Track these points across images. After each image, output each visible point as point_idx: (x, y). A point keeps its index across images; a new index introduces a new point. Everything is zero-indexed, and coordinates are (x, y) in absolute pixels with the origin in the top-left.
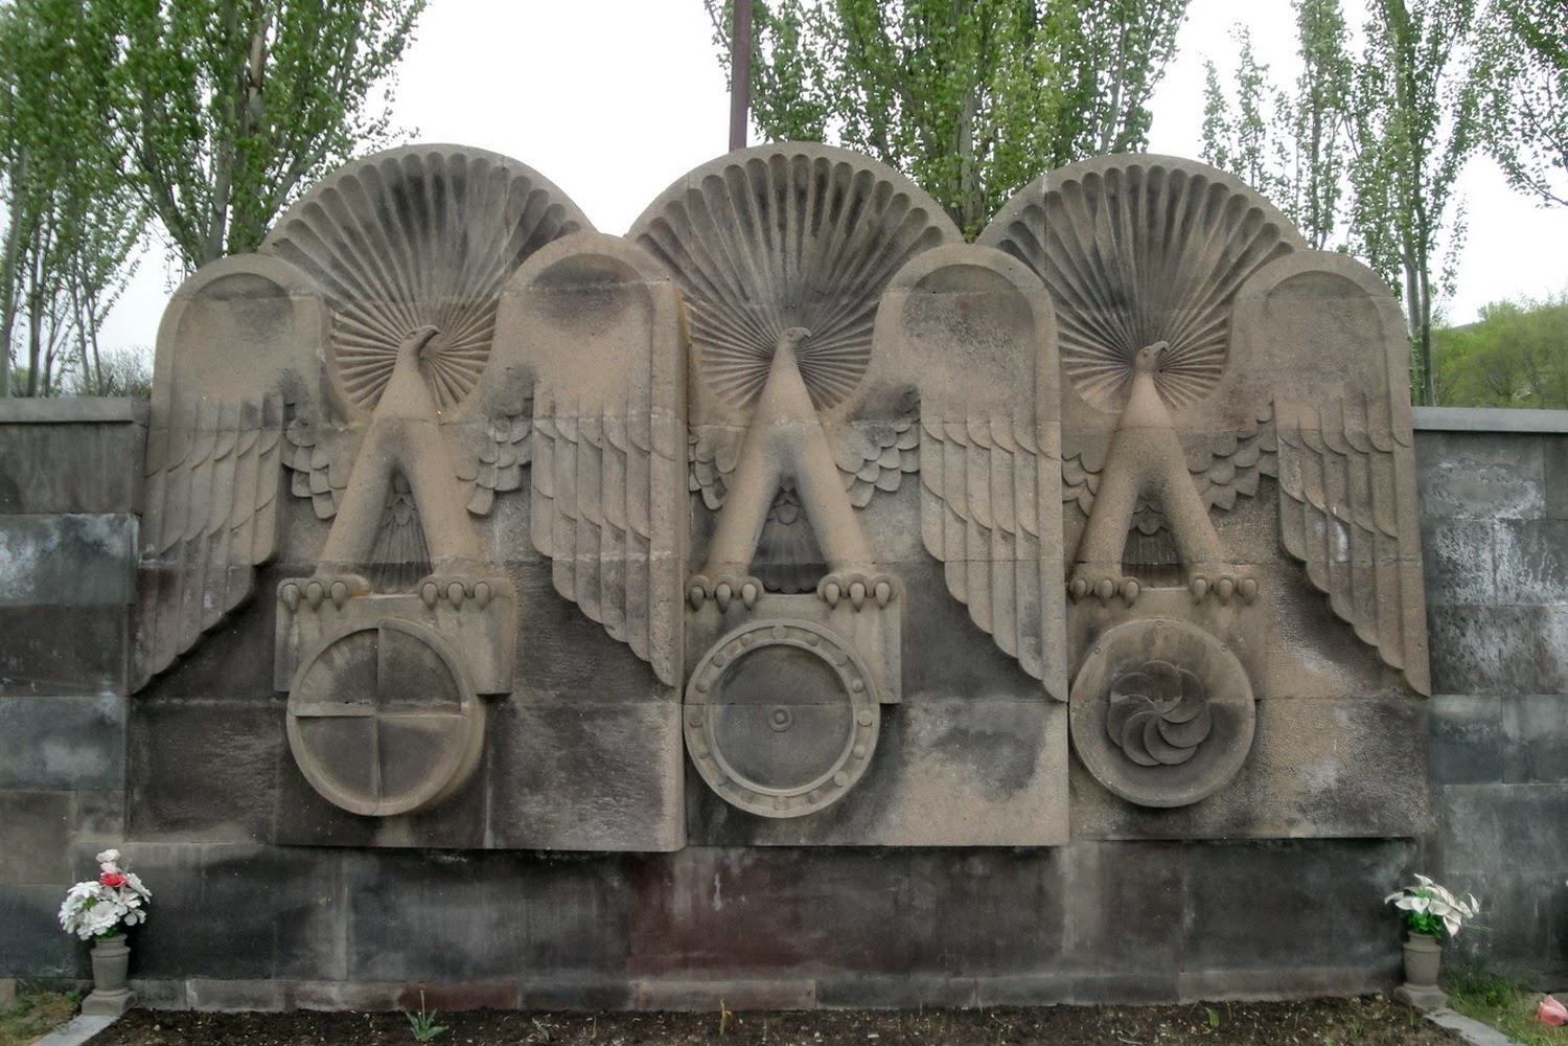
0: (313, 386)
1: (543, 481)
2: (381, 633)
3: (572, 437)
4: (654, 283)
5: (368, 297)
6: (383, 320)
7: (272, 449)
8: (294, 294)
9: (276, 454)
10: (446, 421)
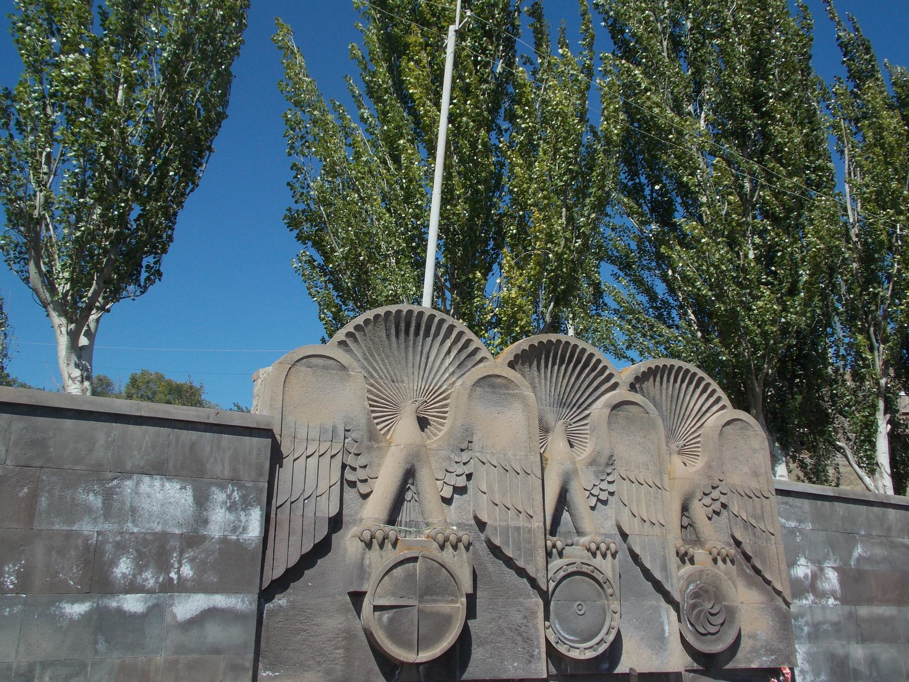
0: (363, 421)
2: (420, 559)
3: (495, 463)
5: (381, 378)
8: (352, 371)
9: (340, 455)
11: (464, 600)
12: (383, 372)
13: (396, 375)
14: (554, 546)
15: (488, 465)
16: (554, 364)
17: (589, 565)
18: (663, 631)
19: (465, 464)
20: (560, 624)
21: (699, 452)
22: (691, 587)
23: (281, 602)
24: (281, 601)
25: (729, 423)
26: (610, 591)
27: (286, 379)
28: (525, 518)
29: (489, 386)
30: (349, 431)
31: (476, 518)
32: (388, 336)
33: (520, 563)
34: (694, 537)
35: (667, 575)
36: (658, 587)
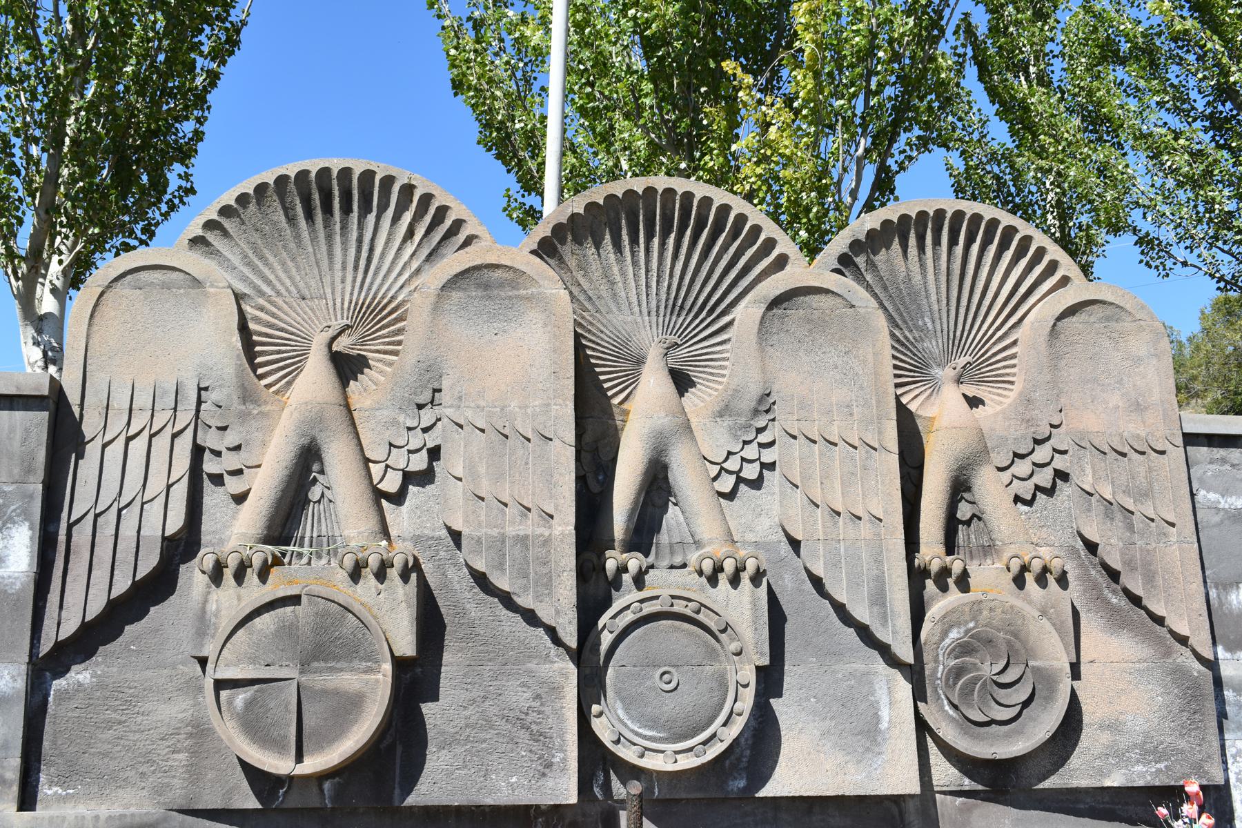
2: (304, 599)
4: (554, 291)
5: (278, 293)
6: (293, 314)
7: (185, 428)
8: (212, 286)
9: (189, 433)
10: (357, 406)
11: (387, 667)
12: (283, 284)
13: (309, 287)
14: (623, 569)
15: (467, 428)
16: (650, 237)
17: (689, 600)
18: (877, 718)
19: (425, 430)
20: (627, 710)
21: (1014, 375)
22: (954, 634)
23: (80, 677)
24: (80, 675)
25: (1072, 311)
26: (734, 647)
27: (94, 311)
28: (537, 519)
29: (478, 286)
30: (206, 389)
31: (449, 529)
32: (291, 220)
33: (524, 601)
34: (985, 541)
35: (885, 612)
36: (865, 633)
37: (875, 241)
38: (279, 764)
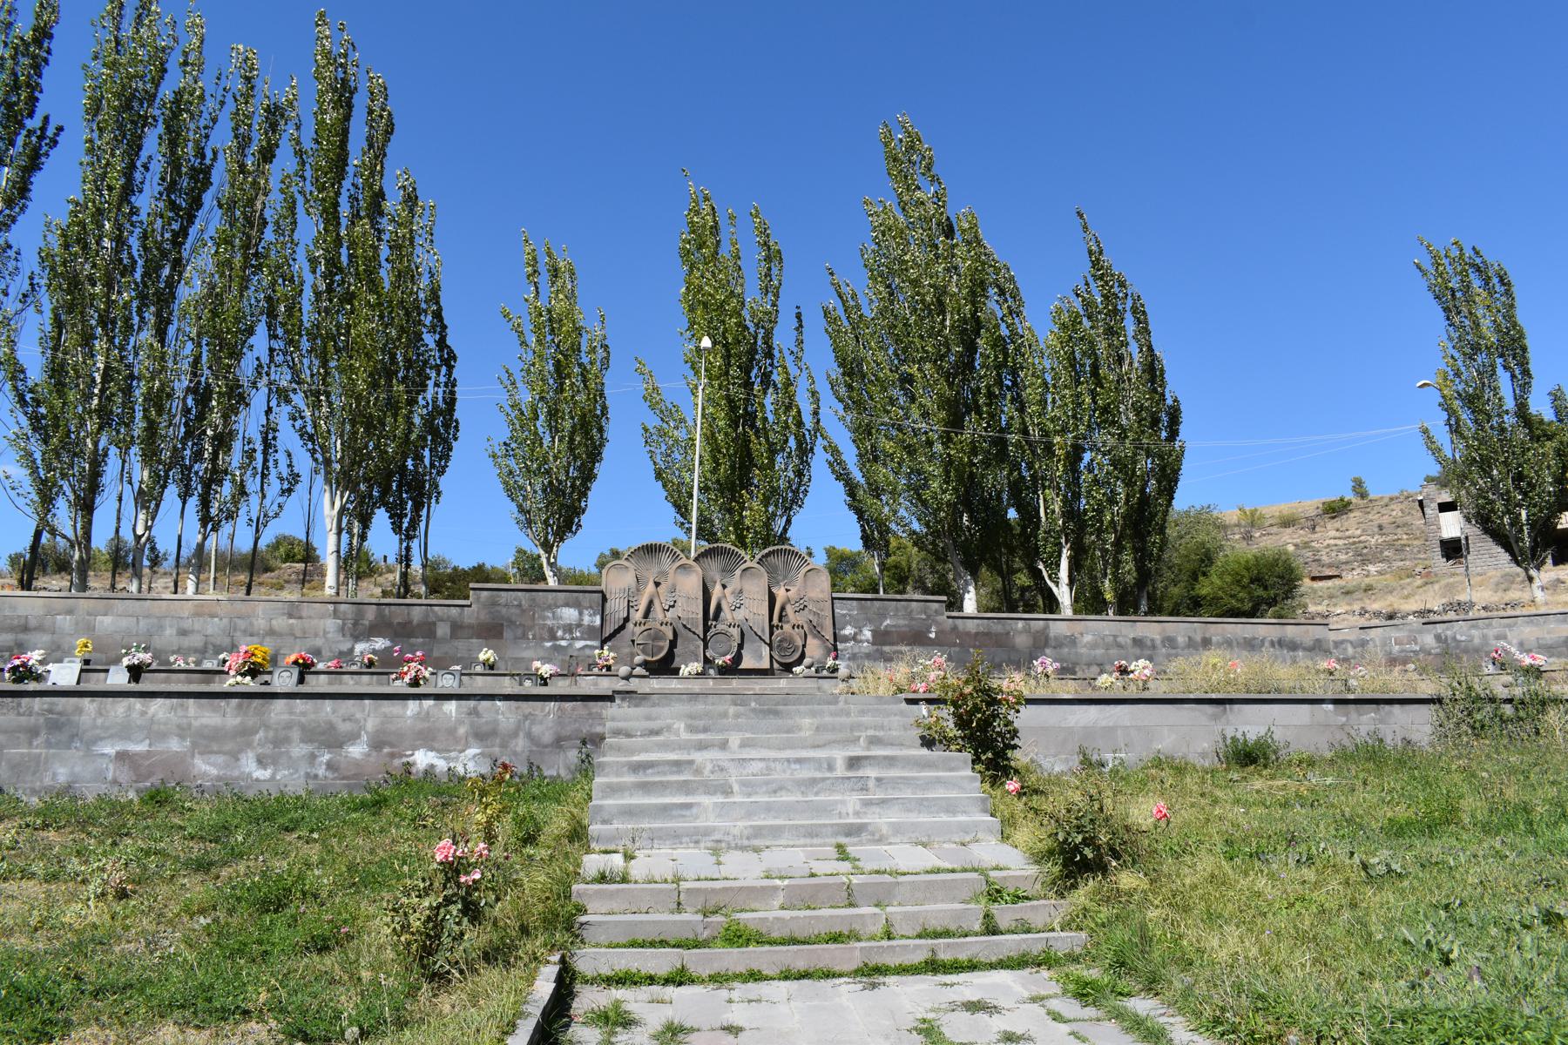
1: (679, 603)
37: (767, 555)
38: (649, 659)
